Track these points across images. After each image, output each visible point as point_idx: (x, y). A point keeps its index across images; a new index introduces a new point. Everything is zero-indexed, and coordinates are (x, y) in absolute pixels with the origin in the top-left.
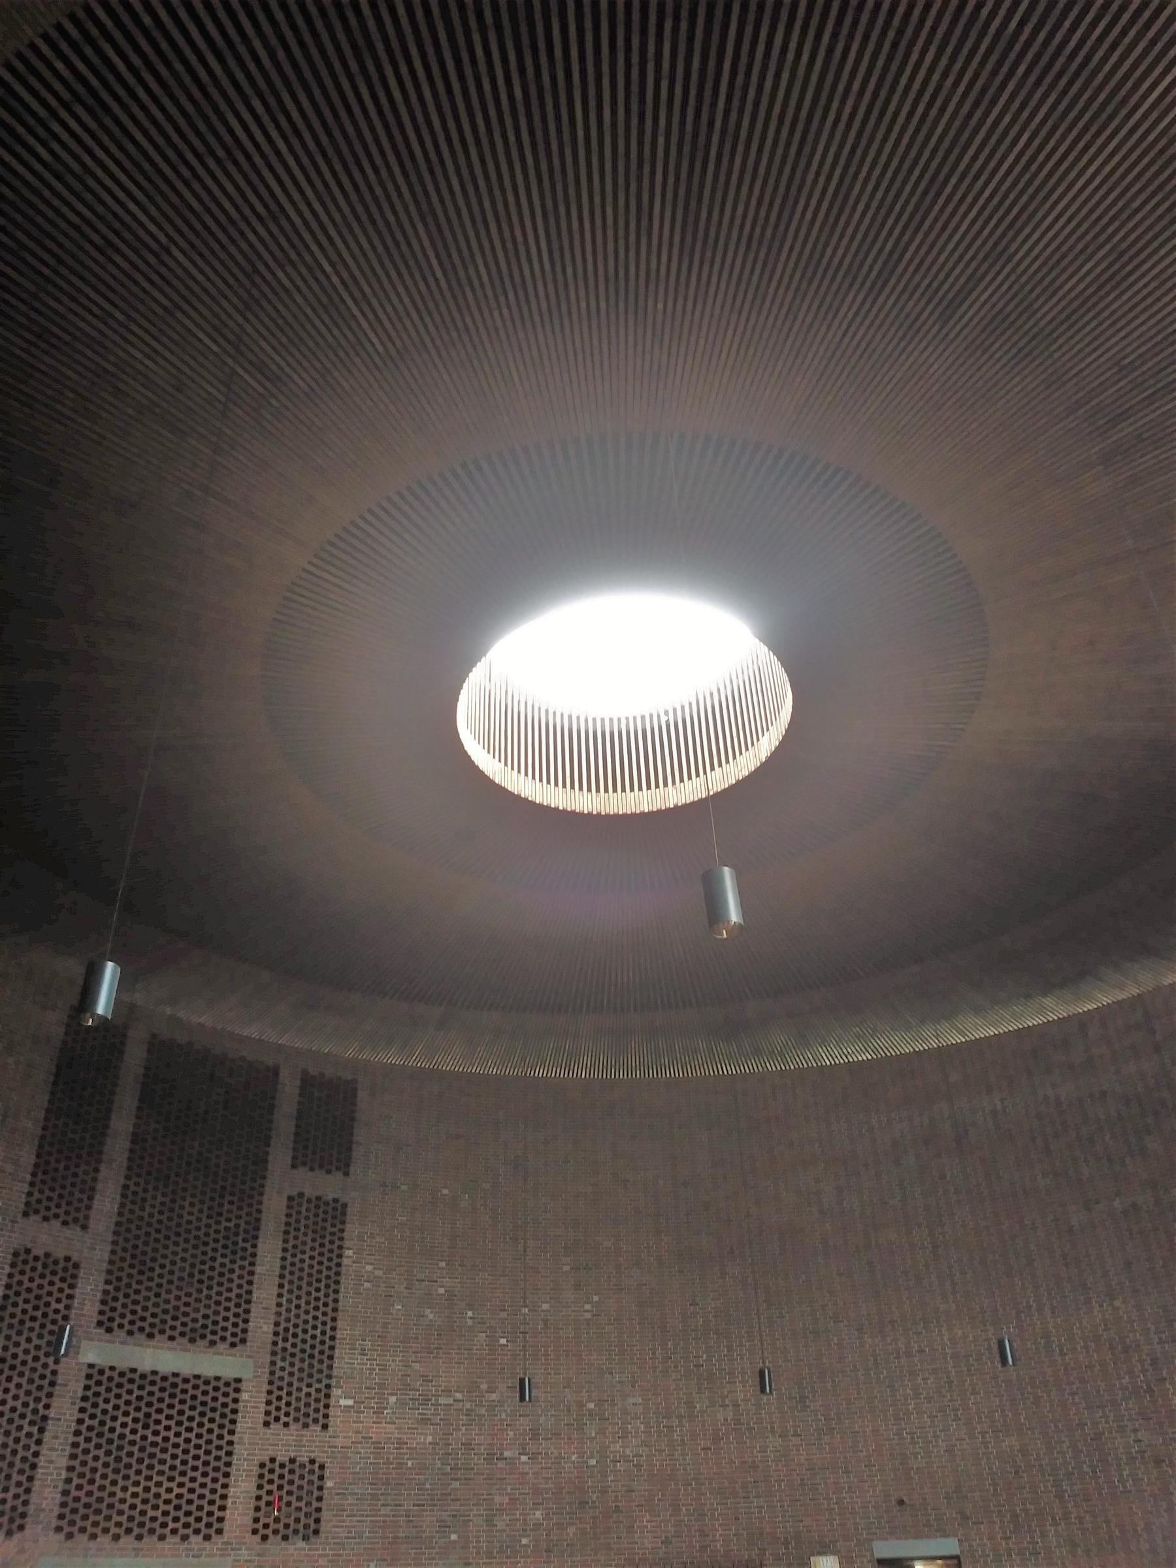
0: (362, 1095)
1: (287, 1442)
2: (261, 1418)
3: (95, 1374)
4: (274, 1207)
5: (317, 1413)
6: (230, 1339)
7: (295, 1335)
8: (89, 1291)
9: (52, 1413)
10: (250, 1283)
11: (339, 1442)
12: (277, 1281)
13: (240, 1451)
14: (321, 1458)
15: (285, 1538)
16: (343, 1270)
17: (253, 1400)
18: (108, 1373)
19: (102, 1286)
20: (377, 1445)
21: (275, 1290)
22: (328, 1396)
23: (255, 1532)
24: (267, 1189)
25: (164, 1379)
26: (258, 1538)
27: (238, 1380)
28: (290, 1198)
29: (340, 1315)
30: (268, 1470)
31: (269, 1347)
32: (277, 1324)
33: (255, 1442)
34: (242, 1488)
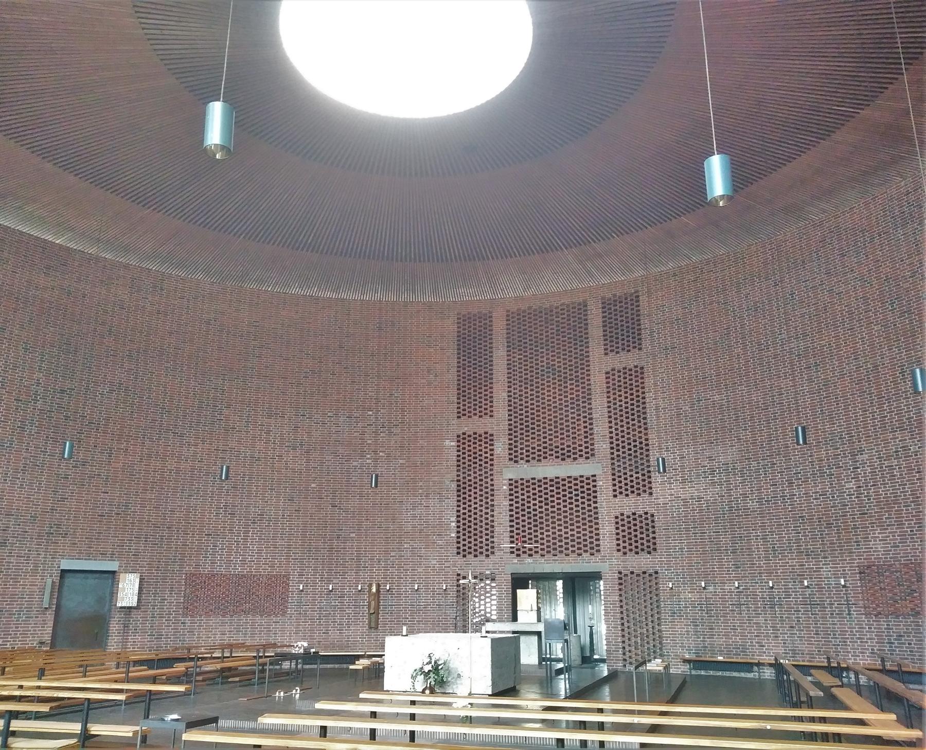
0: (643, 299)
1: (629, 504)
2: (611, 493)
3: (513, 484)
4: (598, 381)
5: (643, 486)
6: (585, 455)
7: (623, 447)
8: (500, 448)
9: (495, 503)
10: (591, 424)
11: (661, 501)
12: (607, 420)
13: (603, 511)
15: (637, 553)
16: (647, 405)
17: (604, 485)
18: (520, 482)
19: (508, 442)
21: (607, 425)
23: (619, 550)
26: (621, 553)
27: (594, 476)
28: (607, 373)
30: (619, 520)
31: (609, 456)
32: (612, 443)
33: (610, 507)
34: (607, 529)
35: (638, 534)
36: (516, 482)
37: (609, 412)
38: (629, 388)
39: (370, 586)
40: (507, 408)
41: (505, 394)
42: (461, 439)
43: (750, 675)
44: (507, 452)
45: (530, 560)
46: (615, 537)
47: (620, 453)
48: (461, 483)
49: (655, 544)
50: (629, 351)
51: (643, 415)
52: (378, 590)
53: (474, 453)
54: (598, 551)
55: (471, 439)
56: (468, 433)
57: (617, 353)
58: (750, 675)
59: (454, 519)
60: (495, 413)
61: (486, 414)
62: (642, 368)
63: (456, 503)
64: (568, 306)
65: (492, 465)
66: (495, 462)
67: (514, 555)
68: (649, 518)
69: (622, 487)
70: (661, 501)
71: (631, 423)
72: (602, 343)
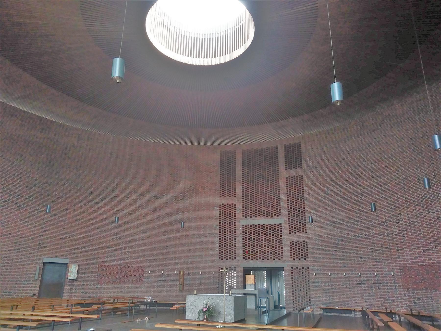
0: (303, 145)
1: (296, 237)
2: (288, 232)
3: (244, 227)
4: (282, 181)
6: (277, 215)
8: (239, 211)
9: (236, 235)
12: (286, 199)
14: (306, 240)
15: (300, 259)
16: (305, 193)
17: (285, 228)
18: (247, 226)
19: (242, 208)
20: (321, 236)
21: (287, 201)
23: (291, 258)
24: (280, 178)
25: (262, 226)
26: (292, 259)
28: (287, 178)
29: (305, 204)
30: (292, 244)
31: (287, 215)
33: (287, 238)
34: (286, 248)
35: (300, 250)
36: (246, 226)
37: (288, 195)
38: (296, 184)
39: (180, 272)
40: (242, 193)
41: (241, 187)
42: (222, 206)
43: (350, 315)
44: (242, 213)
45: (251, 261)
46: (290, 252)
47: (292, 214)
48: (221, 226)
49: (308, 255)
50: (296, 168)
52: (184, 274)
53: (227, 212)
54: (282, 258)
55: (226, 206)
56: (224, 204)
57: (291, 169)
58: (350, 315)
59: (218, 242)
60: (236, 195)
61: (232, 196)
62: (302, 176)
63: (219, 235)
64: (269, 148)
65: (235, 218)
66: (236, 217)
67: (245, 259)
68: (305, 243)
69: (293, 229)
71: (297, 200)
72: (285, 164)
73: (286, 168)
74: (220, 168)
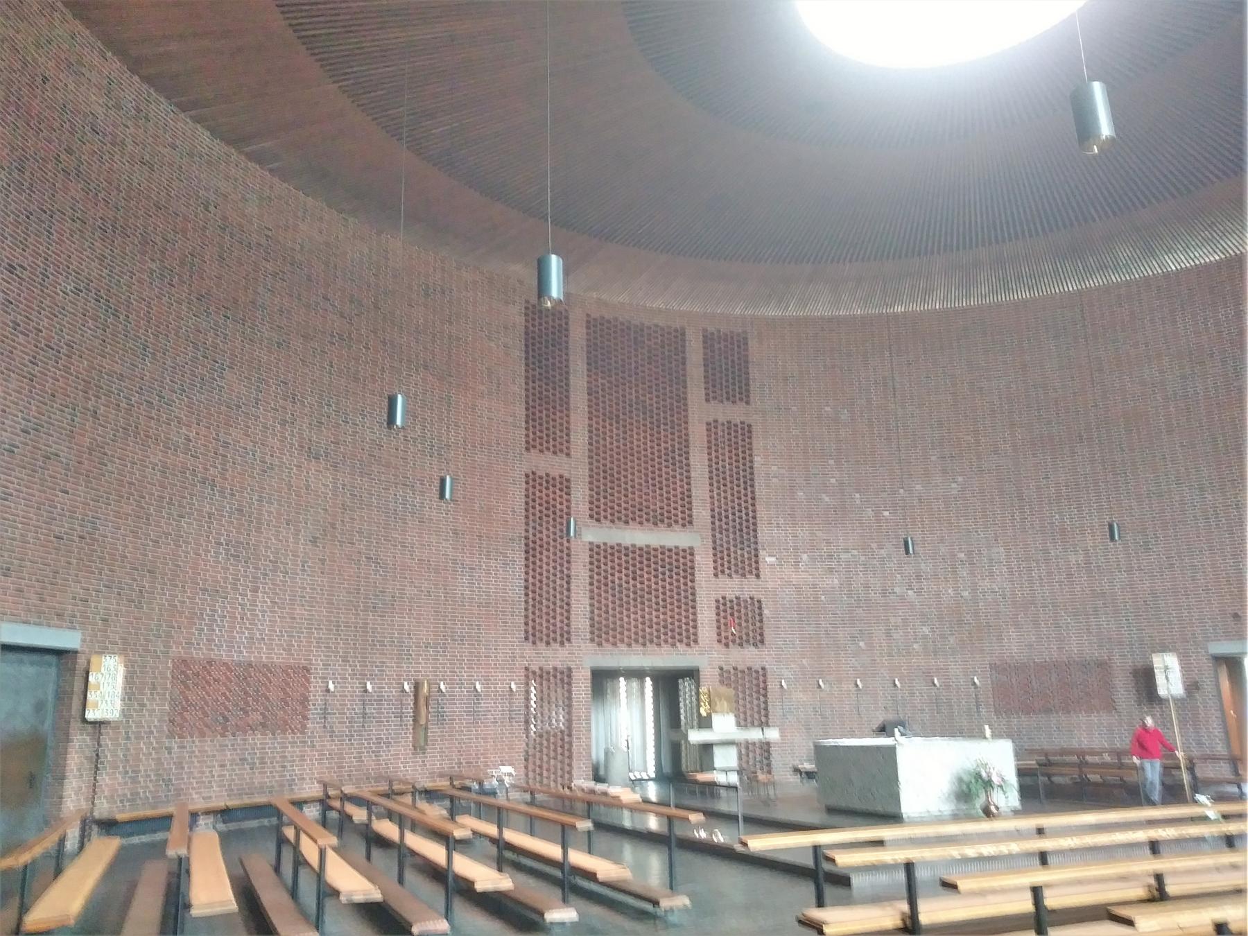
0: (753, 344)
1: (732, 587)
2: (712, 571)
3: (594, 549)
4: (697, 434)
5: (751, 567)
8: (580, 496)
11: (770, 585)
17: (704, 563)
19: (587, 492)
20: (798, 588)
22: (756, 556)
24: (690, 420)
27: (691, 548)
28: (708, 424)
33: (710, 588)
34: (706, 616)
38: (735, 445)
51: (750, 482)
64: (662, 329)
70: (770, 585)
72: (703, 386)
73: (707, 394)
74: (523, 355)
